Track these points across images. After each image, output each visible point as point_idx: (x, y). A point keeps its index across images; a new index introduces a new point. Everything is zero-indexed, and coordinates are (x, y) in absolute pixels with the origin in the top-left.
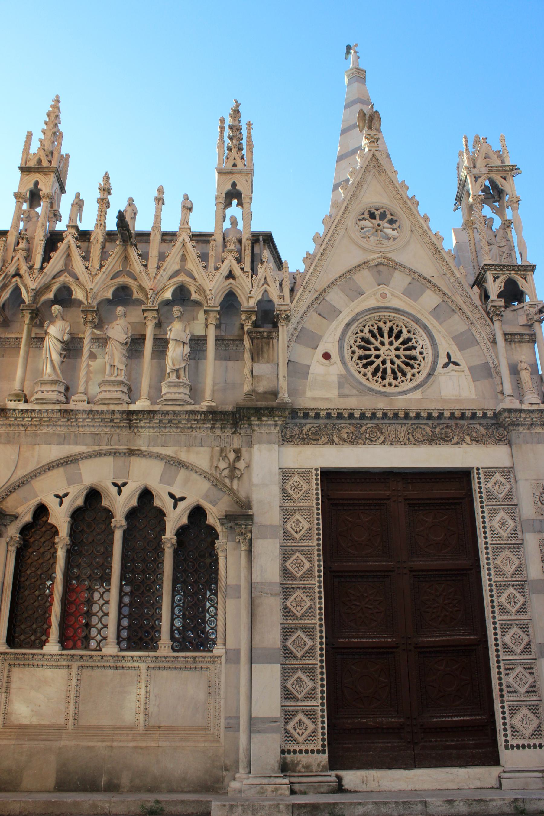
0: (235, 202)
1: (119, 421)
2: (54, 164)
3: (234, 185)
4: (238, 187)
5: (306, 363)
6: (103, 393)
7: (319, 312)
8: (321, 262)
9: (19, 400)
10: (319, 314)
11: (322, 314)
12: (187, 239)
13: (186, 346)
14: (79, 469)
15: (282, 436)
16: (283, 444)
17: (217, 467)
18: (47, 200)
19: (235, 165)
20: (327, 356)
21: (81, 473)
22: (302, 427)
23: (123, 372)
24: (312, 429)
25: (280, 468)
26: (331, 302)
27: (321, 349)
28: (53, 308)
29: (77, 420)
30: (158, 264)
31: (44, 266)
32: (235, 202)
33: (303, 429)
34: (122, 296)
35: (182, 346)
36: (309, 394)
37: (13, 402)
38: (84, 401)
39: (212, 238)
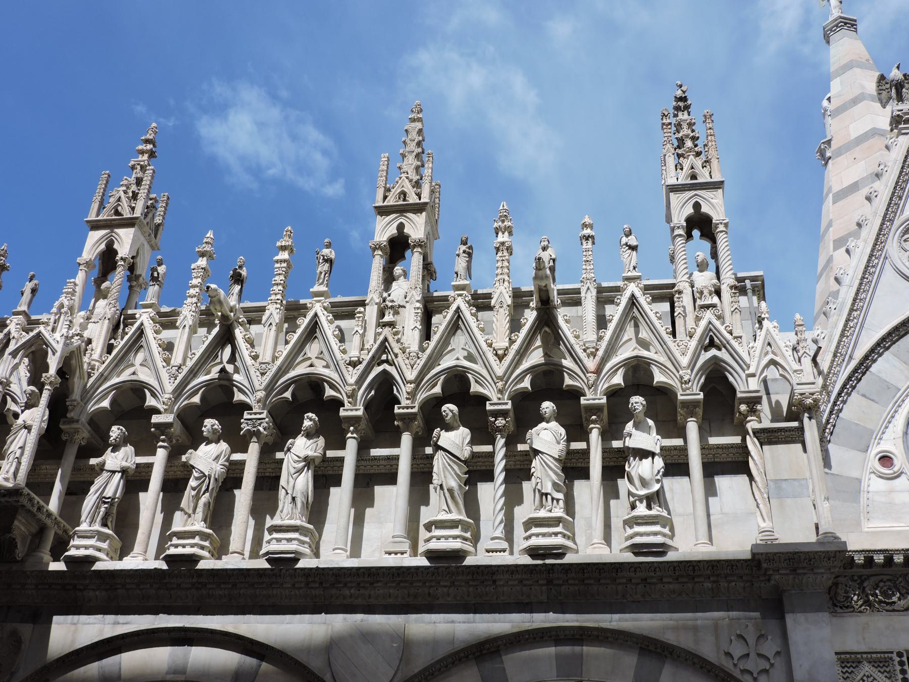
0: (696, 233)
1: (561, 582)
2: (425, 198)
3: (697, 206)
4: (705, 209)
5: (855, 474)
6: (534, 538)
7: (862, 392)
8: (855, 314)
9: (402, 553)
10: (864, 396)
11: (868, 395)
12: (638, 293)
13: (656, 458)
14: (502, 662)
15: (831, 598)
16: (836, 612)
17: (728, 654)
18: (419, 250)
19: (694, 177)
20: (886, 460)
21: (504, 669)
22: (862, 582)
23: (561, 502)
24: (881, 584)
25: (836, 653)
26: (880, 375)
27: (875, 451)
28: (444, 408)
29: (494, 582)
30: (598, 334)
31: (425, 345)
32: (696, 233)
33: (865, 584)
34: (549, 383)
35: (650, 458)
36: (867, 526)
37: (393, 555)
38: (504, 551)
39: (676, 289)
